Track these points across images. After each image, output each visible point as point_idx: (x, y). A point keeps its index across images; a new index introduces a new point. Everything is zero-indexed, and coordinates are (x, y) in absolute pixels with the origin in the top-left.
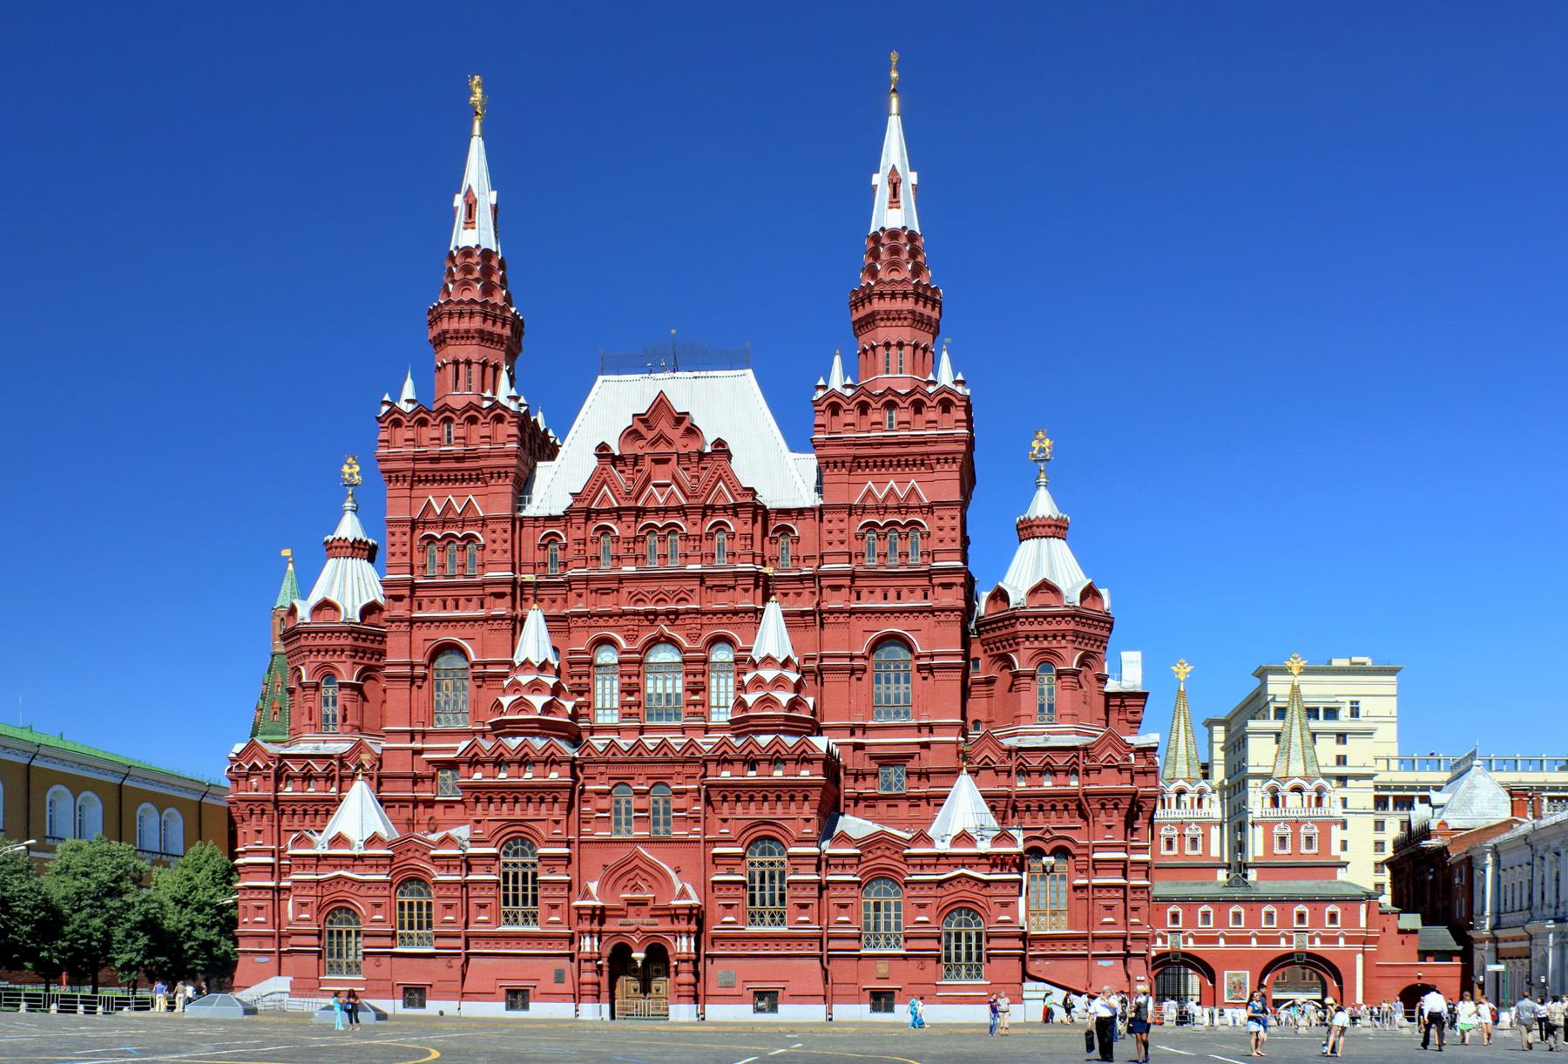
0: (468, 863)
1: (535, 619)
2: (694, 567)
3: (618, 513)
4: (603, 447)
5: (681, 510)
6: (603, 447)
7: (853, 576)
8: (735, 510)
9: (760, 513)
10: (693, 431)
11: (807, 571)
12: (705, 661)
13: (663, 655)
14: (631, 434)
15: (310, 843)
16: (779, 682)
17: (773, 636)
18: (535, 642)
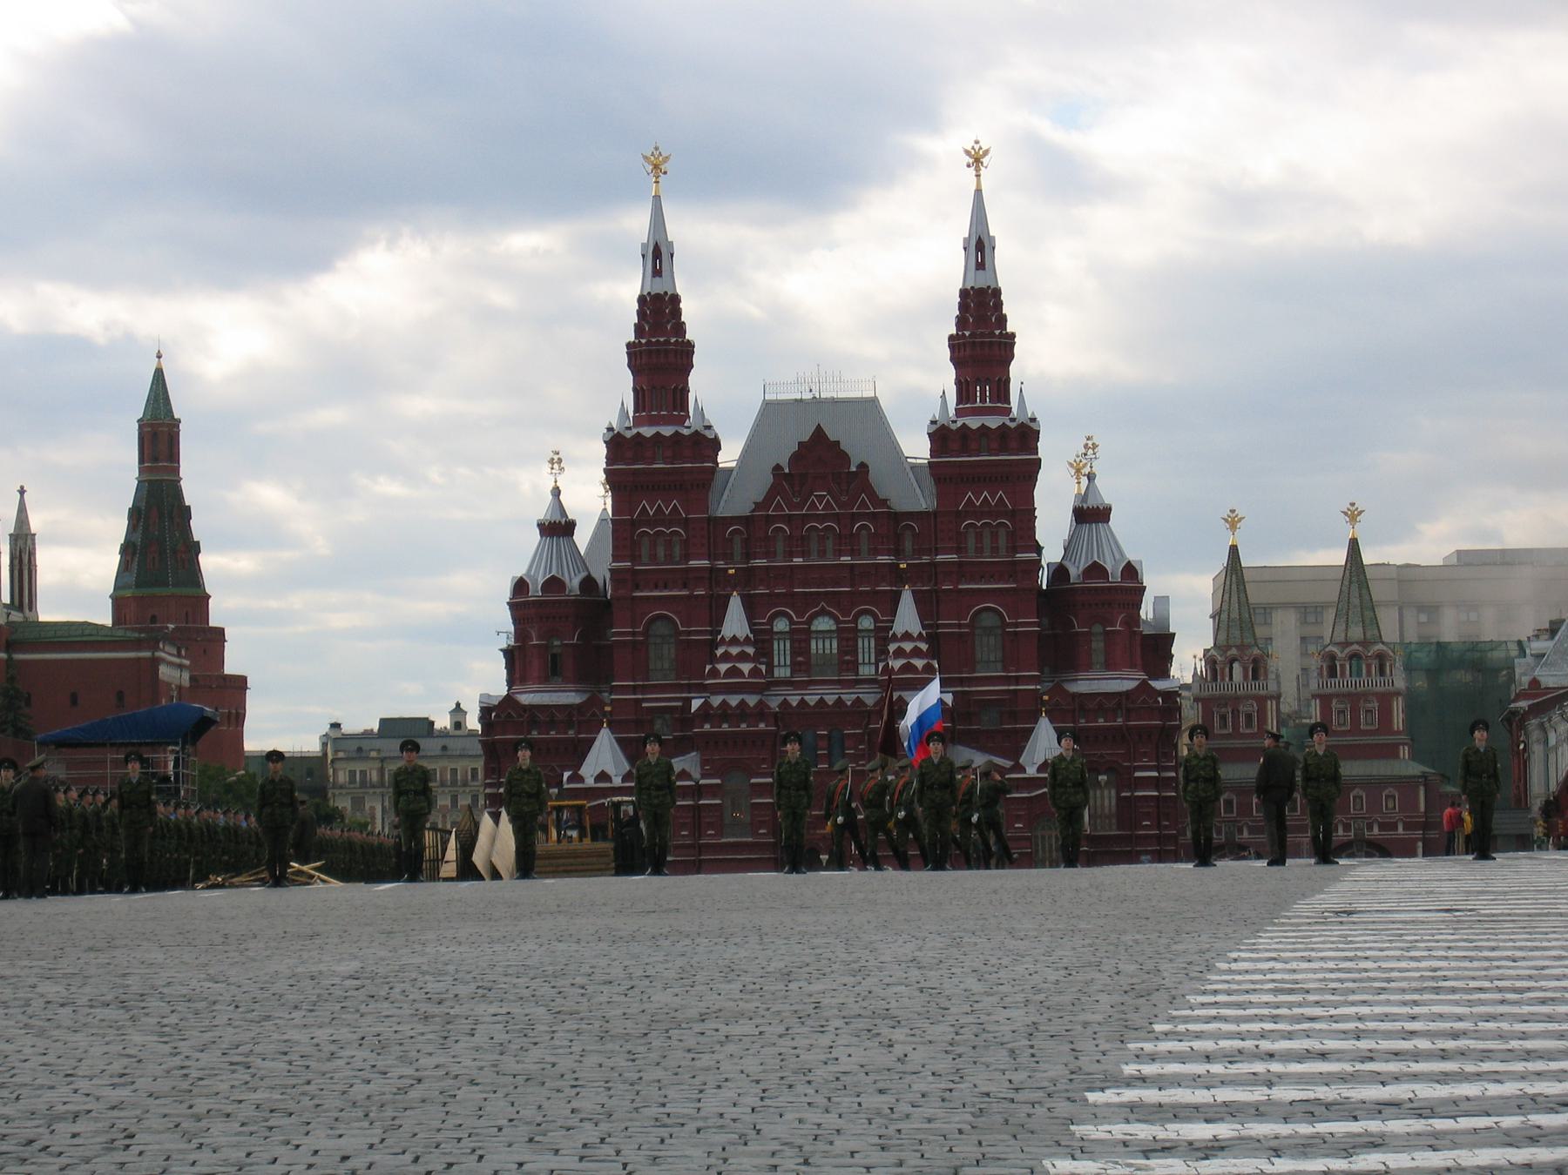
0: (698, 791)
1: (735, 608)
2: (846, 559)
3: (788, 519)
4: (778, 468)
5: (837, 518)
6: (778, 468)
7: (960, 564)
8: (873, 517)
9: (898, 517)
10: (844, 458)
11: (926, 559)
12: (856, 630)
13: (823, 624)
14: (795, 458)
15: (581, 780)
16: (916, 652)
17: (907, 618)
18: (735, 622)
